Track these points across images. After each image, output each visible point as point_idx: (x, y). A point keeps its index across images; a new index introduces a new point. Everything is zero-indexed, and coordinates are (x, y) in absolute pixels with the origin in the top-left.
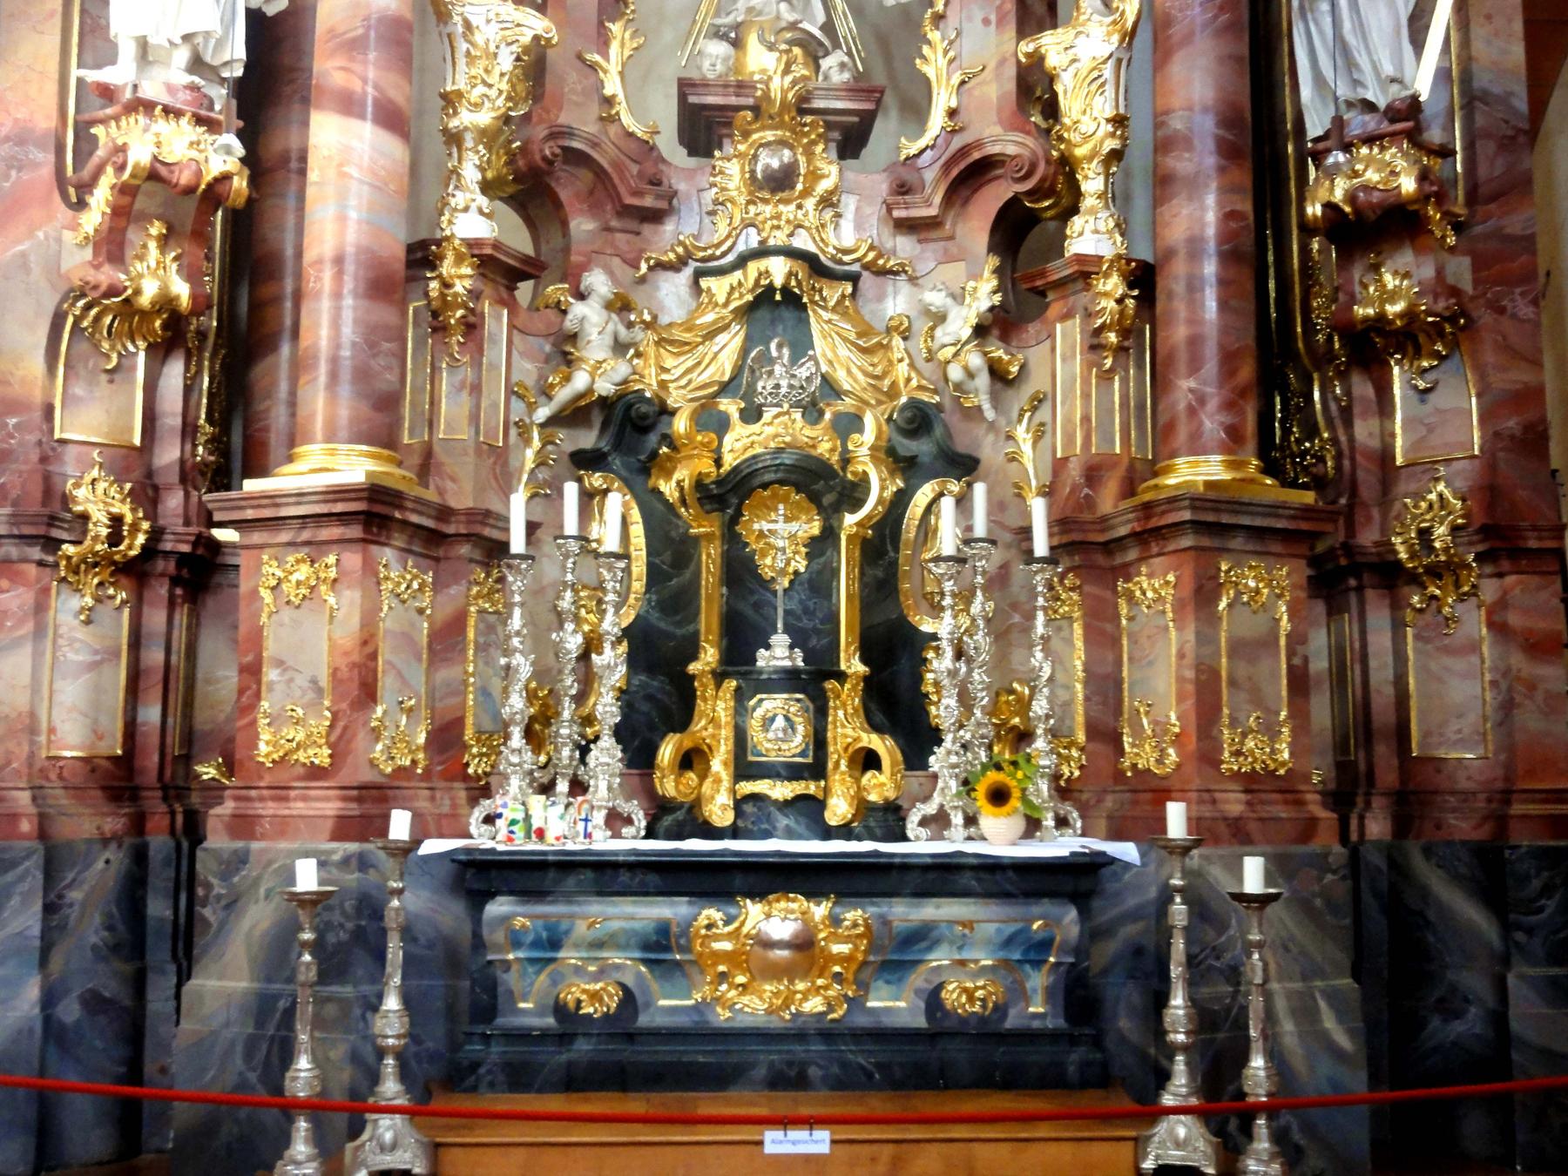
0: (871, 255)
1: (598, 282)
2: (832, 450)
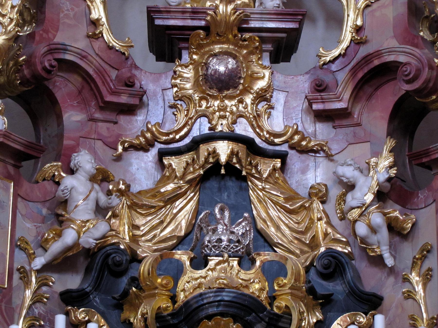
0: (297, 138)
1: (84, 160)
2: (262, 290)
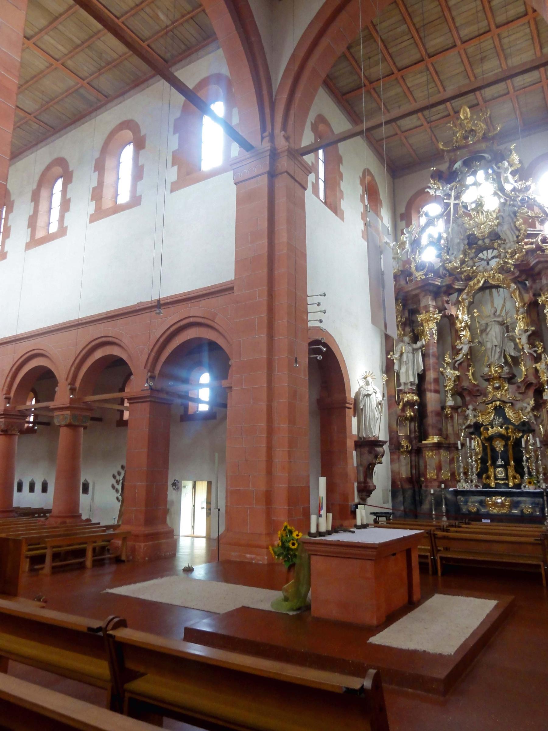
1: (471, 407)
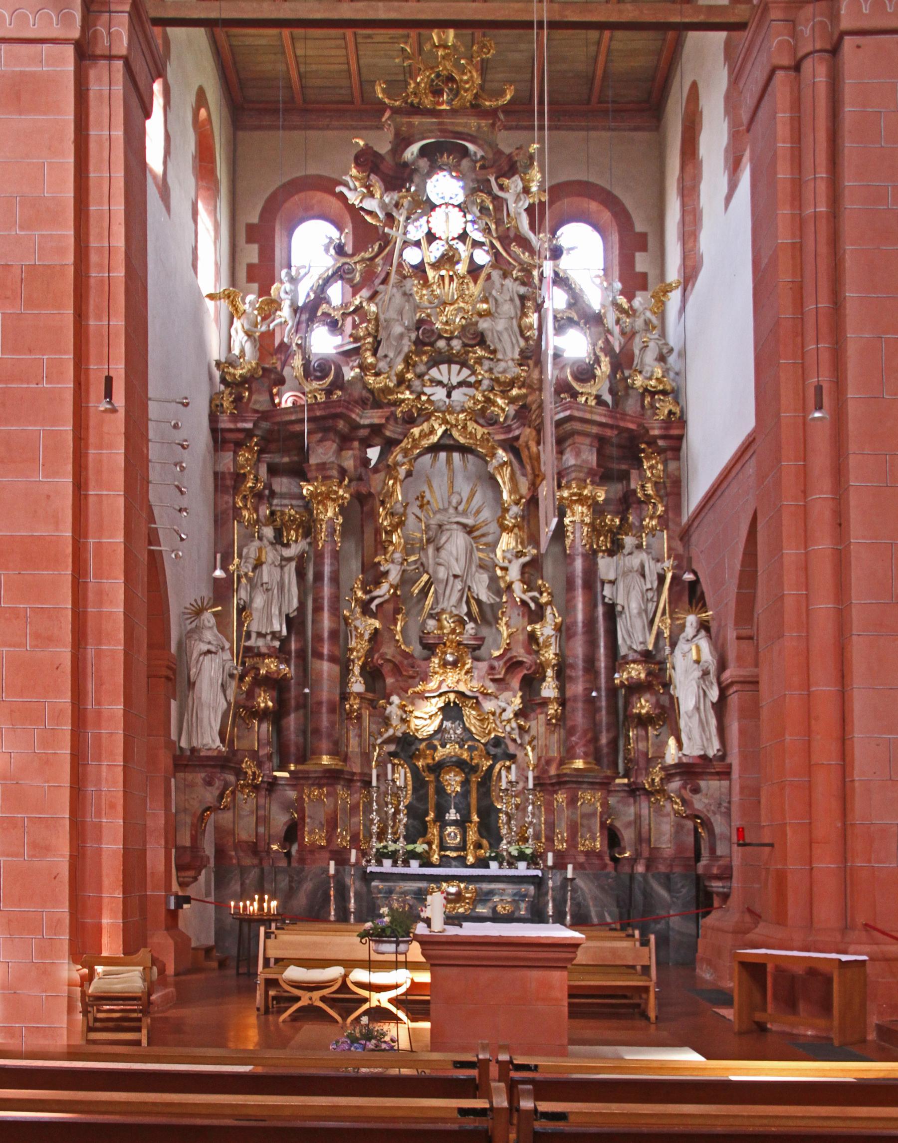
1: (395, 699)
